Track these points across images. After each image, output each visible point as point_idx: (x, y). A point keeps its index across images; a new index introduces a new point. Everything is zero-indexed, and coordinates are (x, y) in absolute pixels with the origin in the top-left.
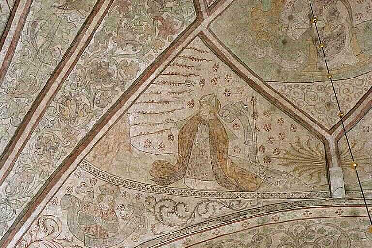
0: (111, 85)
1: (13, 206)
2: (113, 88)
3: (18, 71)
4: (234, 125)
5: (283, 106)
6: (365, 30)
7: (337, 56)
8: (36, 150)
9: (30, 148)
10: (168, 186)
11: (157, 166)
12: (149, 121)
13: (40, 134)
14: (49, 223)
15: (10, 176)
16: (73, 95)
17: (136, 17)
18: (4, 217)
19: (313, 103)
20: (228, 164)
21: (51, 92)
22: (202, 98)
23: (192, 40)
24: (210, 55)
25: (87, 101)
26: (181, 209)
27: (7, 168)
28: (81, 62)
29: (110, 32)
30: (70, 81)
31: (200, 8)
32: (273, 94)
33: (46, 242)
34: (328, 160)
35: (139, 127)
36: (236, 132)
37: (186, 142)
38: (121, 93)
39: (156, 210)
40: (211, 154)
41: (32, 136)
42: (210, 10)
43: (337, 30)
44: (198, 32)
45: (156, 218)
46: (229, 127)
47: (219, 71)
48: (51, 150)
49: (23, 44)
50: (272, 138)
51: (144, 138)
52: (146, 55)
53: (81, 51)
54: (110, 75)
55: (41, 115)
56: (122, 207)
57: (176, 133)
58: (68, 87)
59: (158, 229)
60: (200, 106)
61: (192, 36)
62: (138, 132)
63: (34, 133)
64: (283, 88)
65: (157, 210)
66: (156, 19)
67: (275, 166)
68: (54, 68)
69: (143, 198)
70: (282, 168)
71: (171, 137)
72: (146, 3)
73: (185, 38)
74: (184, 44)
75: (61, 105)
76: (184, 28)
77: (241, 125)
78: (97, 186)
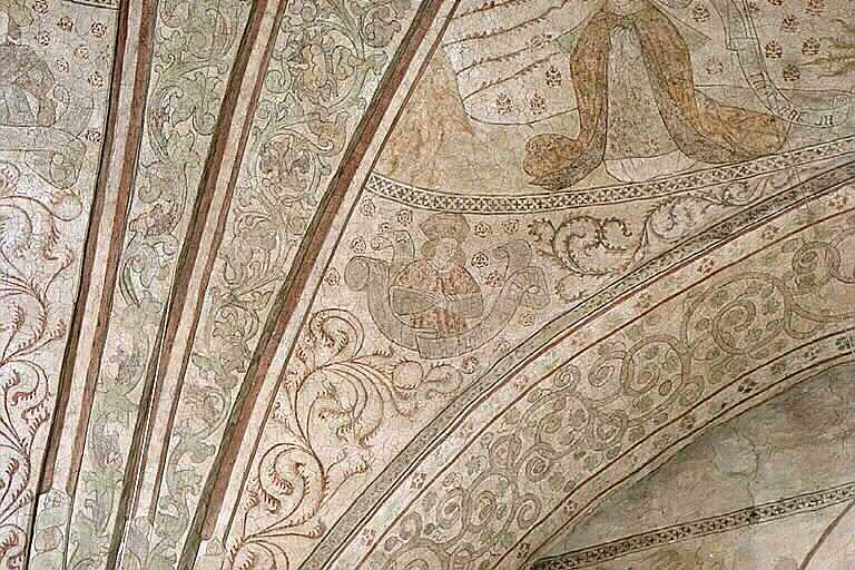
1: (249, 306)
3: (179, 10)
4: (695, 12)
8: (265, 176)
9: (252, 177)
10: (574, 188)
11: (538, 149)
12: (496, 53)
13: (264, 139)
14: (334, 327)
15: (225, 243)
16: (312, 34)
18: (237, 333)
20: (700, 107)
25: (345, 41)
26: (613, 231)
27: (214, 227)
33: (338, 367)
35: (475, 73)
36: (704, 28)
37: (592, 82)
39: (557, 247)
40: (656, 91)
41: (249, 146)
45: (564, 266)
46: (684, 19)
48: (297, 168)
51: (493, 94)
56: (481, 259)
57: (562, 64)
58: (297, 20)
59: (575, 286)
62: (476, 84)
63: (251, 139)
65: (560, 246)
67: (812, 80)
69: (523, 229)
70: (832, 83)
71: (552, 77)
77: (711, 9)
78: (415, 223)
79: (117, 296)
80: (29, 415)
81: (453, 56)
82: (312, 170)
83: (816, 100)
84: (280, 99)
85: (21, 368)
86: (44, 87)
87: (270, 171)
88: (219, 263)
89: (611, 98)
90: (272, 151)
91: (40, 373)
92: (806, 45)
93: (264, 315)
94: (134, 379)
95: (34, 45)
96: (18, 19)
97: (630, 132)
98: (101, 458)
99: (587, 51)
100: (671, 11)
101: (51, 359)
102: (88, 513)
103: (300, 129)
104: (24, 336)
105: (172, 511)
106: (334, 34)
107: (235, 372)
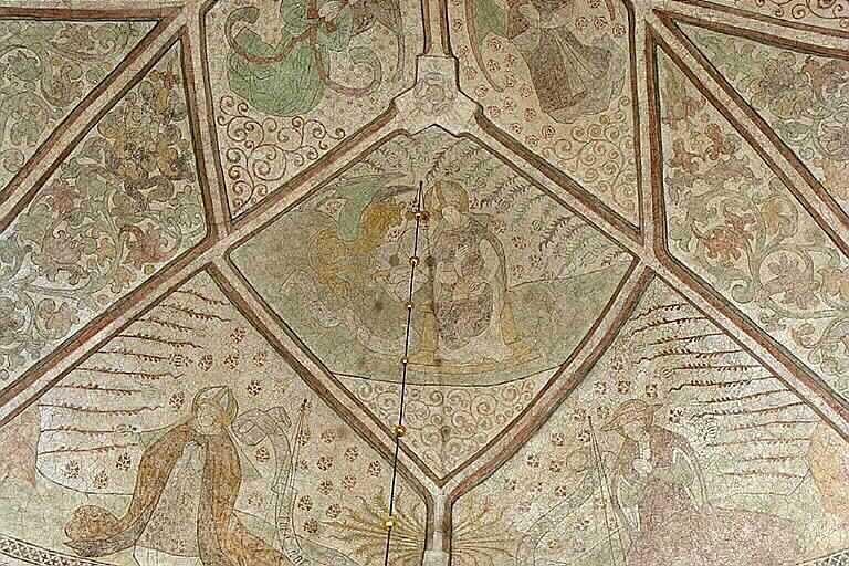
0: (11, 347)
2: (17, 351)
4: (258, 452)
5: (359, 422)
6: (526, 299)
7: (473, 340)
11: (83, 516)
12: (84, 426)
17: (87, 220)
19: (419, 424)
20: (231, 527)
22: (202, 391)
23: (190, 277)
24: (228, 311)
29: (27, 243)
31: (213, 218)
32: (343, 399)
34: (428, 536)
35: (58, 436)
36: (261, 467)
37: (154, 476)
38: (31, 363)
42: (232, 223)
43: (479, 292)
44: (205, 262)
47: (243, 343)
50: (329, 484)
51: (65, 459)
52: (94, 295)
54: (13, 325)
57: (137, 455)
60: (195, 408)
61: (190, 269)
62: (56, 445)
64: (367, 391)
66: (125, 228)
67: (325, 541)
71: (124, 461)
72: (110, 199)
73: (176, 271)
74: (173, 282)
76: (181, 251)
77: (272, 454)
81: (46, 415)
83: (320, 554)
89: (164, 496)
92: (330, 508)
97: (167, 529)
99: (161, 452)
100: (241, 444)
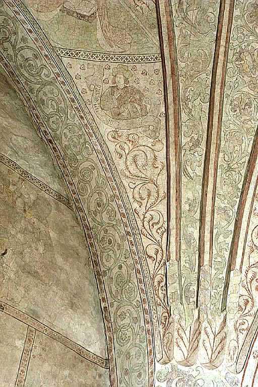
8: (233, 113)
9: (228, 115)
15: (222, 146)
16: (243, 47)
18: (233, 182)
21: (221, 57)
28: (236, 12)
30: (235, 36)
41: (225, 103)
48: (247, 107)
49: (179, 28)
53: (230, 4)
55: (222, 83)
58: (236, 43)
63: (225, 100)
68: (215, 33)
75: (237, 63)
79: (183, 177)
80: (159, 231)
82: (253, 106)
84: (235, 79)
85: (152, 213)
86: (140, 100)
87: (235, 111)
88: (221, 155)
90: (235, 102)
91: (160, 213)
93: (243, 172)
94: (196, 209)
95: (135, 85)
96: (127, 76)
98: (188, 243)
101: (162, 208)
102: (187, 265)
103: (246, 90)
104: (152, 200)
105: (219, 259)
106: (253, 44)
107: (235, 199)
